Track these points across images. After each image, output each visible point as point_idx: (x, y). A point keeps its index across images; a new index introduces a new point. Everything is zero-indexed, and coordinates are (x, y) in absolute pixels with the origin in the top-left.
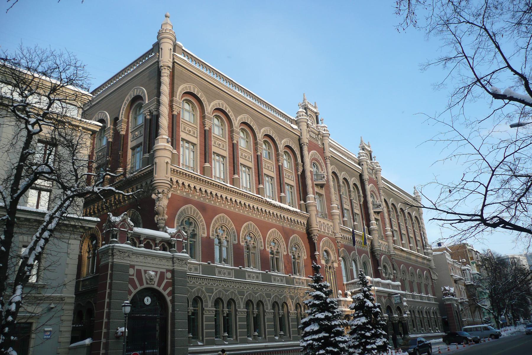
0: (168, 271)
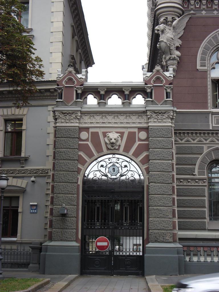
0: (140, 129)
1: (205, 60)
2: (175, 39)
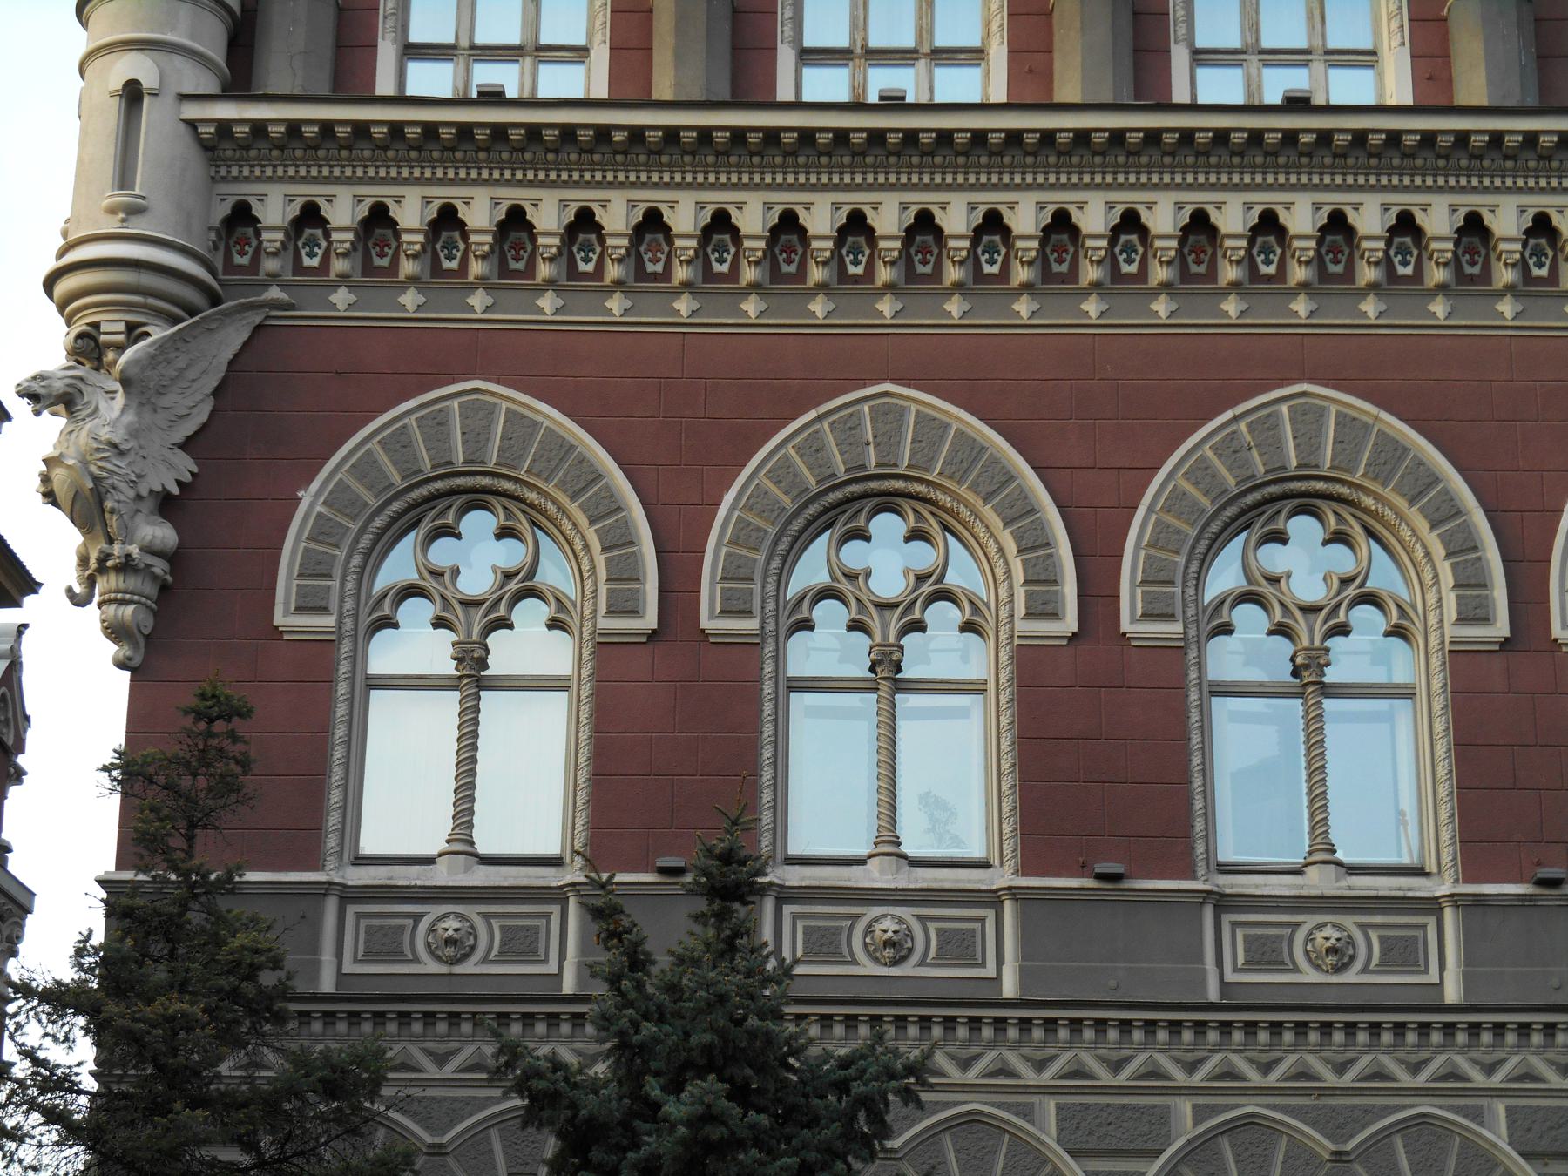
1: (329, 576)
2: (141, 447)
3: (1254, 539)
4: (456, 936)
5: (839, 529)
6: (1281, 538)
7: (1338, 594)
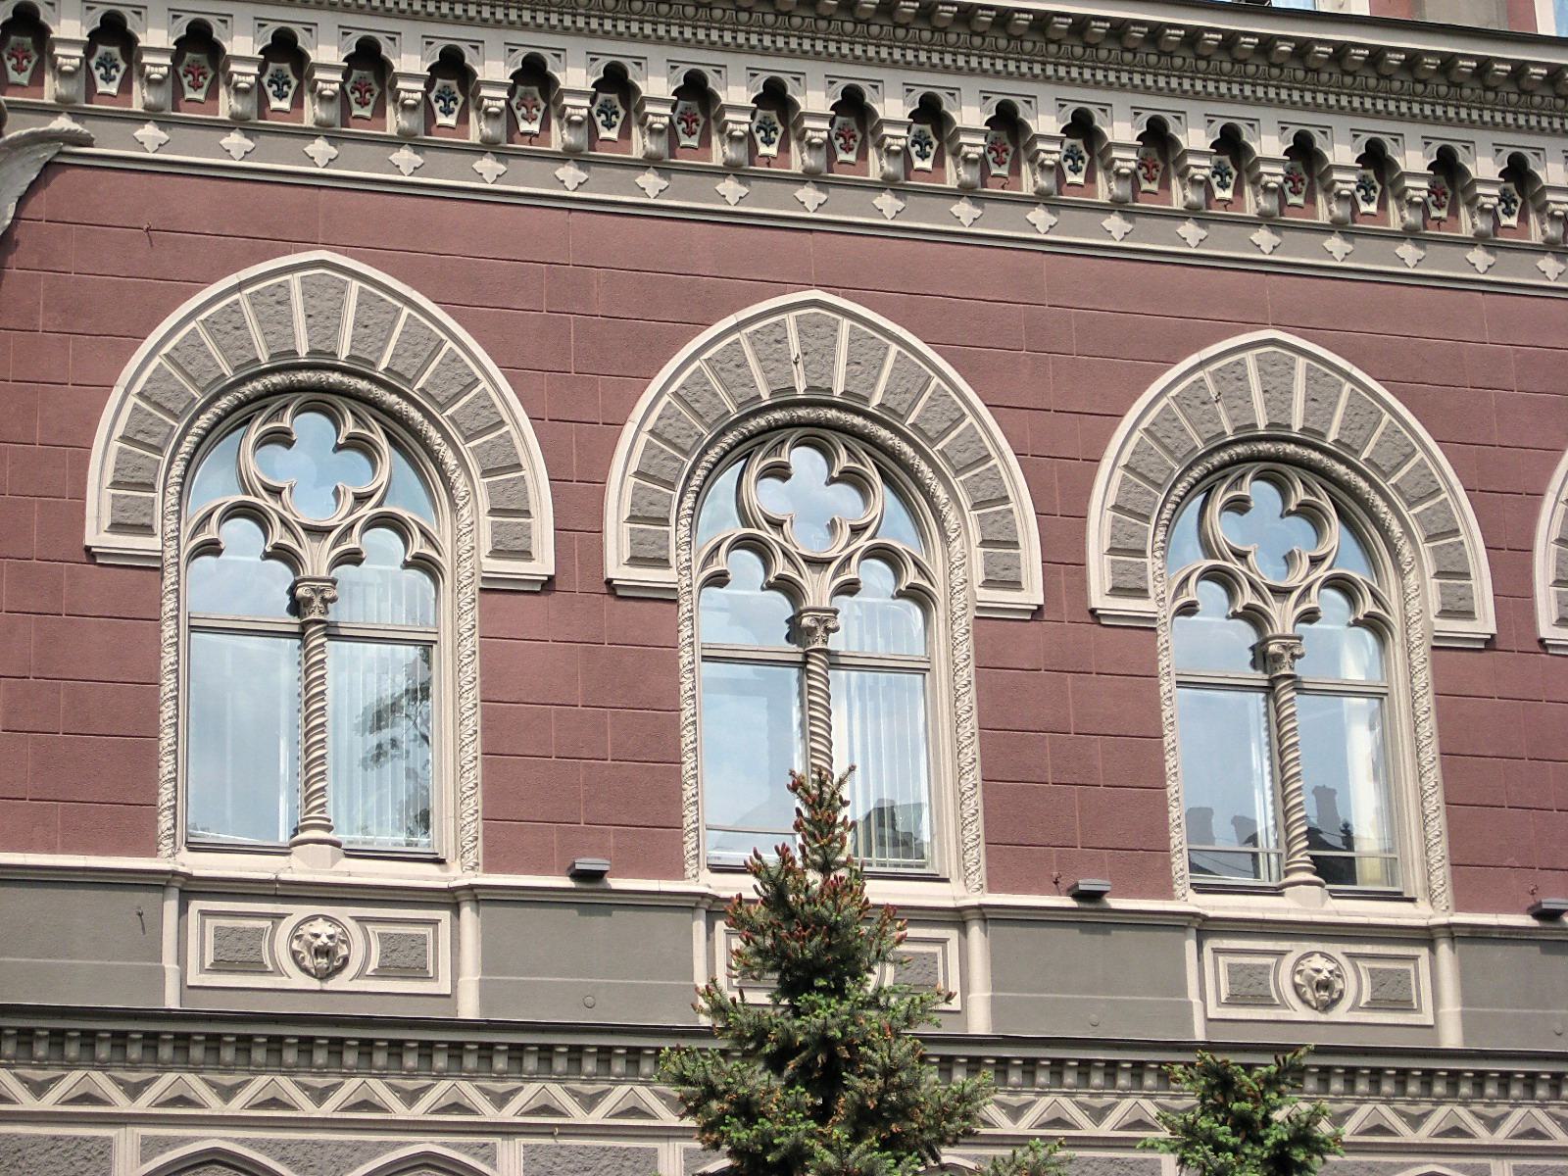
1: (151, 487)
3: (253, 437)
4: (330, 944)
5: (256, 430)
6: (283, 438)
7: (351, 513)
